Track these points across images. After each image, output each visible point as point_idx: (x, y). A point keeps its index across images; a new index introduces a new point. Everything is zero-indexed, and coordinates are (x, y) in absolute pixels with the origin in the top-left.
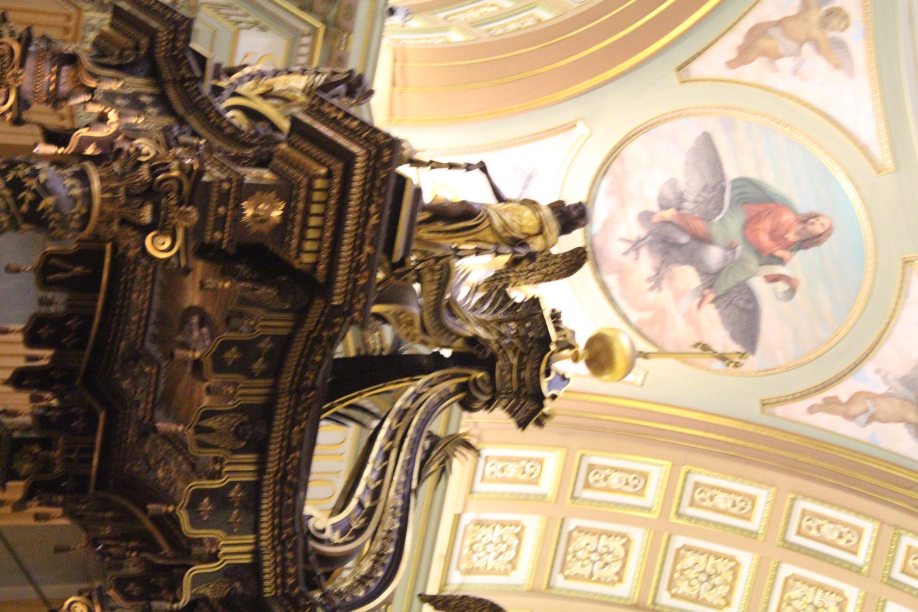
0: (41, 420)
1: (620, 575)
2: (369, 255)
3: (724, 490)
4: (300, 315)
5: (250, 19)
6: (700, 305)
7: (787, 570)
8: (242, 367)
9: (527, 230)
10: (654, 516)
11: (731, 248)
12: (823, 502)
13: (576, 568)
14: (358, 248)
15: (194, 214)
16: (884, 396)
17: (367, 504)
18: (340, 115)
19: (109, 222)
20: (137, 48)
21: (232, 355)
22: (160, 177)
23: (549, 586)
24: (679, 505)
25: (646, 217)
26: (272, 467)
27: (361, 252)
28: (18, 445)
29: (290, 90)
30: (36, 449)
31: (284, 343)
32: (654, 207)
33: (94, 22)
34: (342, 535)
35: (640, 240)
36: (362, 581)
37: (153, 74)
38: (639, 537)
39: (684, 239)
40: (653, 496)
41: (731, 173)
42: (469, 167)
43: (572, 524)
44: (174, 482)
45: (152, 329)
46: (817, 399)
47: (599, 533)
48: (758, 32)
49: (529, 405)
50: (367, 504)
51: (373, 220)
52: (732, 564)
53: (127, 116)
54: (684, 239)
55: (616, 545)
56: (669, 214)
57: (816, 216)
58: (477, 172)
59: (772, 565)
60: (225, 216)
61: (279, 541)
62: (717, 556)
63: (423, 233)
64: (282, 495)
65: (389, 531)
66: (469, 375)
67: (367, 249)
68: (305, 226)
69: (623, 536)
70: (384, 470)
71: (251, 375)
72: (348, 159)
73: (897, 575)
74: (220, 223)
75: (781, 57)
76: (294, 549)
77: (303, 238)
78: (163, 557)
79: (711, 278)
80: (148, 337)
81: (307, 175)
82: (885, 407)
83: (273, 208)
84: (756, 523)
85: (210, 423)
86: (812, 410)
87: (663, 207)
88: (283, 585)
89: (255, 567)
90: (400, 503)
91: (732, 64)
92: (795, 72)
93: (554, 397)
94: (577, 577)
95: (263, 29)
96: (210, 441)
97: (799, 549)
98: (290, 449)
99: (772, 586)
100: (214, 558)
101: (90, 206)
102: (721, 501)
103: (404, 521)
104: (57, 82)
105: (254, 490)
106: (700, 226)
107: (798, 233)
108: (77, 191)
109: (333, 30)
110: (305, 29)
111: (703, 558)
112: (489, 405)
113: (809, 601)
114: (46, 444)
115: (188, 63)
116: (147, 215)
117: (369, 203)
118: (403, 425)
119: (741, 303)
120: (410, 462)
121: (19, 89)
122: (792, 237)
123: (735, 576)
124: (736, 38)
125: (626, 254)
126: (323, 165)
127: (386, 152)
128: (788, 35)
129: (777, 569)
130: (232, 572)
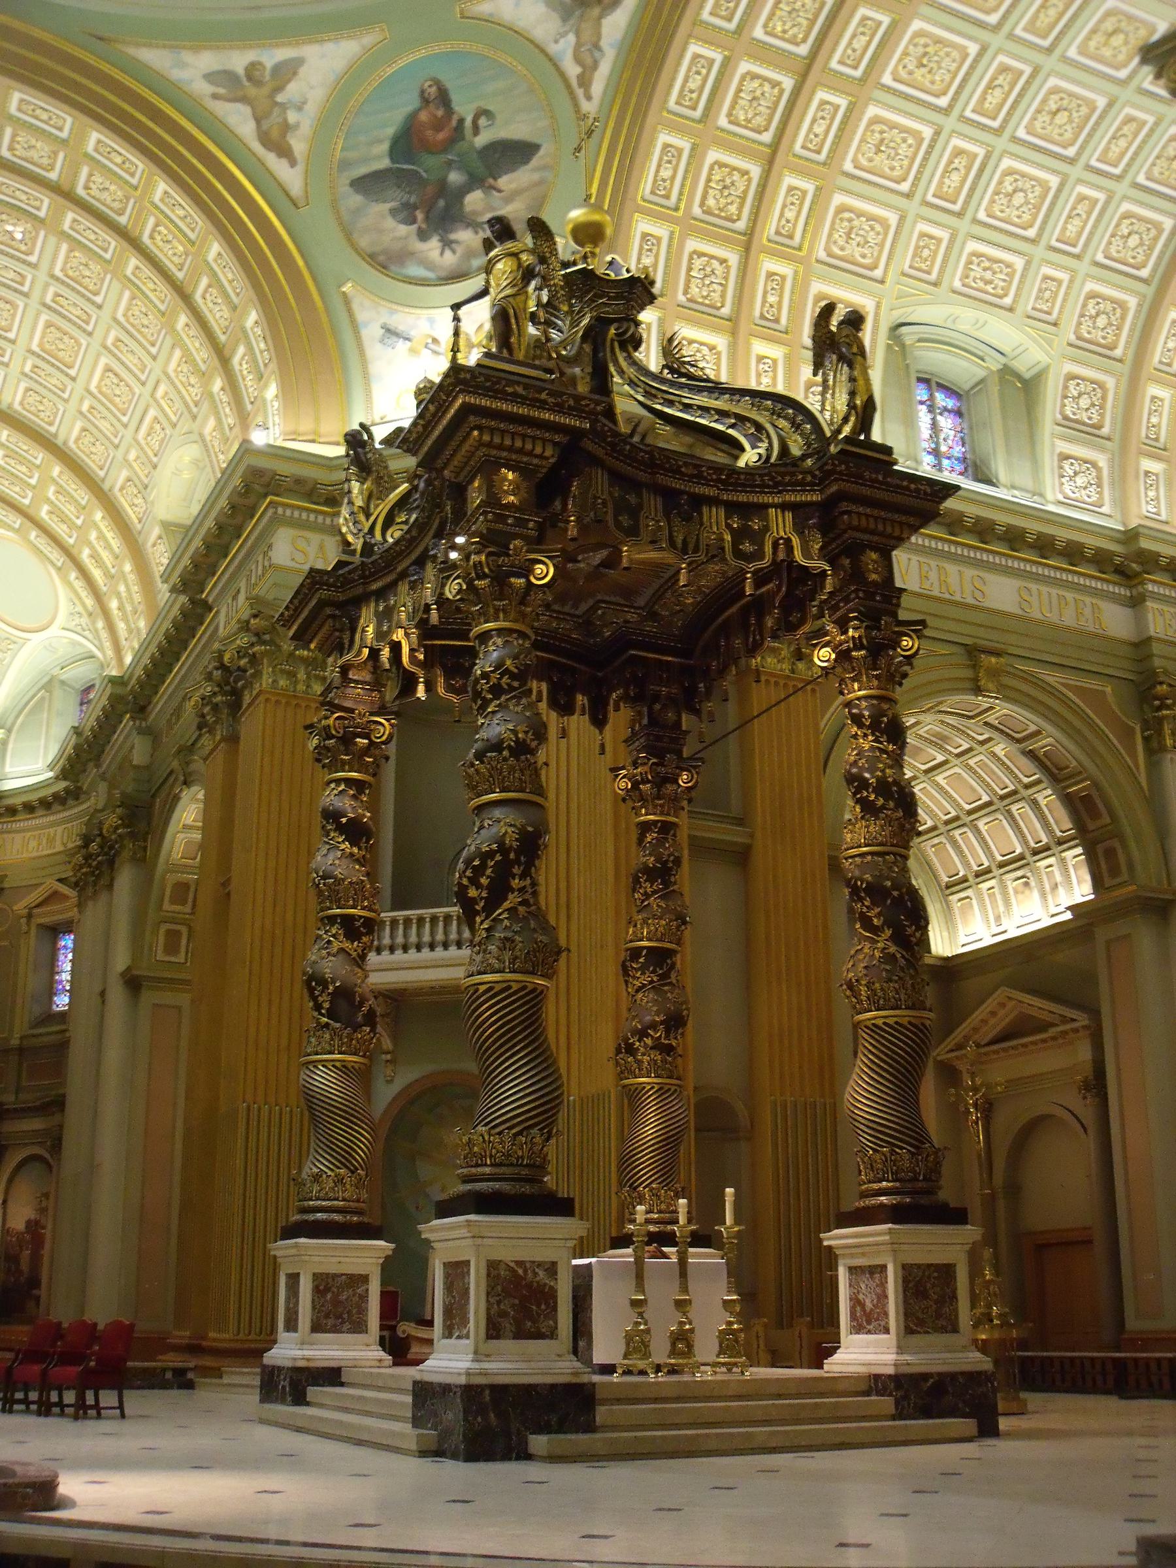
0: (633, 700)
1: (723, 261)
3: (657, 171)
4: (596, 461)
5: (260, 558)
6: (500, 191)
7: (723, 121)
8: (635, 512)
9: (515, 268)
10: (677, 229)
11: (449, 164)
12: (671, 86)
13: (716, 296)
14: (542, 405)
16: (578, 34)
18: (422, 422)
19: (524, 615)
20: (333, 616)
21: (625, 520)
22: (486, 570)
24: (668, 208)
25: (423, 236)
27: (545, 402)
28: (653, 722)
29: (361, 492)
30: (657, 707)
31: (616, 477)
32: (415, 227)
34: (762, 441)
35: (442, 240)
36: (796, 426)
37: (358, 601)
38: (692, 244)
39: (441, 203)
40: (660, 230)
41: (385, 163)
42: (457, 319)
43: (681, 298)
44: (699, 587)
45: (567, 609)
46: (580, 92)
47: (689, 278)
48: (265, 139)
49: (638, 290)
51: (520, 390)
52: (716, 167)
53: (399, 620)
54: (441, 203)
55: (698, 263)
56: (420, 216)
57: (423, 92)
58: (462, 312)
59: (718, 133)
61: (777, 487)
62: (709, 180)
63: (520, 355)
64: (736, 484)
65: (753, 404)
66: (612, 340)
67: (543, 396)
68: (521, 451)
69: (691, 258)
70: (700, 408)
71: (640, 506)
72: (466, 409)
73: (732, 26)
74: (520, 522)
75: (285, 120)
76: (783, 475)
78: (779, 587)
79: (475, 181)
80: (572, 611)
81: (477, 449)
82: (587, 36)
83: (505, 479)
84: (685, 144)
85: (679, 539)
86: (589, 98)
87: (414, 221)
88: (812, 484)
90: (727, 396)
91: (293, 163)
92: (300, 109)
93: (628, 271)
94: (723, 296)
95: (270, 546)
96: (694, 540)
97: (707, 109)
98: (699, 476)
99: (735, 134)
100: (788, 541)
101: (510, 631)
102: (666, 173)
103: (744, 392)
104: (362, 683)
106: (430, 190)
107: (438, 108)
108: (499, 641)
110: (270, 512)
111: (711, 191)
112: (637, 324)
113: (748, 104)
114: (656, 698)
116: (520, 582)
118: (660, 395)
119: (497, 156)
121: (372, 714)
122: (440, 113)
123: (726, 166)
124: (271, 159)
125: (454, 252)
126: (469, 434)
127: (462, 376)
128: (267, 115)
129: (723, 130)
130: (799, 528)
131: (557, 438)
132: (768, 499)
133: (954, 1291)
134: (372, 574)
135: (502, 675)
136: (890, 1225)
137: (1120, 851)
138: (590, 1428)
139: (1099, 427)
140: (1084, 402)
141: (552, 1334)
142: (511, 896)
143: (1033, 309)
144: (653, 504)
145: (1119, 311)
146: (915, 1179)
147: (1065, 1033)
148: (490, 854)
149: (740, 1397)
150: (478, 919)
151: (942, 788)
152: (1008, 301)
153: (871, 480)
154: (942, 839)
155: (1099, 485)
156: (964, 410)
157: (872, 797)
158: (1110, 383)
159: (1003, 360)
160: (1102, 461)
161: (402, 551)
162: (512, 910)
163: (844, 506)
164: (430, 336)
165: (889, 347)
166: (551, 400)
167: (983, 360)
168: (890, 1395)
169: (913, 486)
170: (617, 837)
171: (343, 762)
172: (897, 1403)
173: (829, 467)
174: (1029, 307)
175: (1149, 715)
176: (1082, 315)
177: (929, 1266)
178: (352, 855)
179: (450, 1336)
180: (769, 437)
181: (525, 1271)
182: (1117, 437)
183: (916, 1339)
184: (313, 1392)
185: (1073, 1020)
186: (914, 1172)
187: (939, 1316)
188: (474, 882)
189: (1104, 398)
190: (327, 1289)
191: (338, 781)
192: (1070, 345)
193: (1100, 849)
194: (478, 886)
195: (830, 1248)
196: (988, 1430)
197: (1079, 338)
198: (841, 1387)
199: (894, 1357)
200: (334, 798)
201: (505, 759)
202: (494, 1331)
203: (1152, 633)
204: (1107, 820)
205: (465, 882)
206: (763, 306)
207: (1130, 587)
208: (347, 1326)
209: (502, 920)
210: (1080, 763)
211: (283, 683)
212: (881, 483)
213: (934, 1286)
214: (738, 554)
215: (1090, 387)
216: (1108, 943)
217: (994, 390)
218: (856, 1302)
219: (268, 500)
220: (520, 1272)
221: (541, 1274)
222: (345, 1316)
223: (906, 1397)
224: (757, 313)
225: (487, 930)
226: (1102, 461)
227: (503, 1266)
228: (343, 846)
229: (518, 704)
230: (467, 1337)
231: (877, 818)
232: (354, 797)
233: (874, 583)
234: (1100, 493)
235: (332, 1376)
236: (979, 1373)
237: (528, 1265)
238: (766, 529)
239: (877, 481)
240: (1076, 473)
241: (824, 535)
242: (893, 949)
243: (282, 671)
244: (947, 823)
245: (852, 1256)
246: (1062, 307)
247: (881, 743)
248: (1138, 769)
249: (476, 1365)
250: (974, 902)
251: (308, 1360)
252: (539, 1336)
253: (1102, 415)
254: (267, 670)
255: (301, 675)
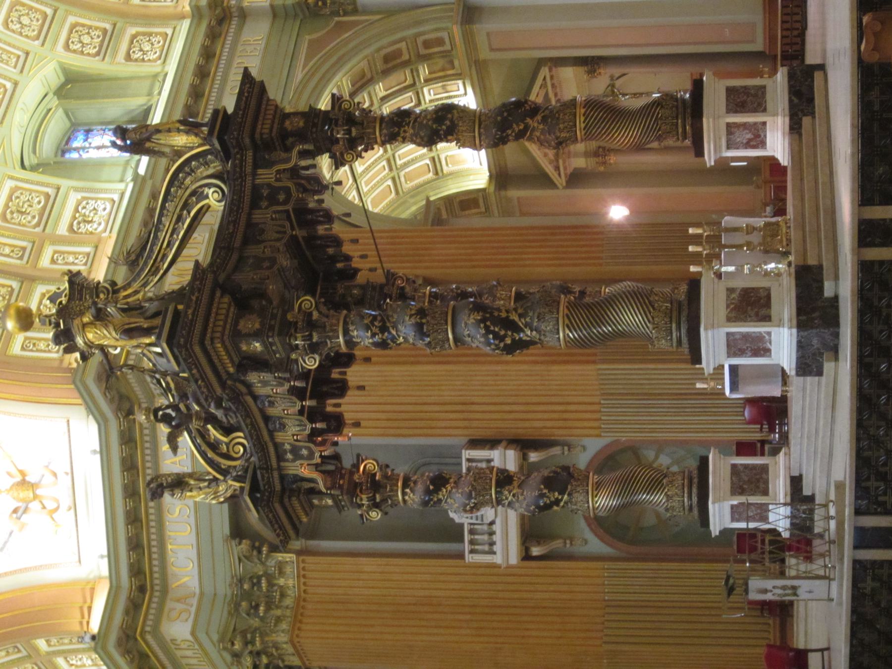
2: (193, 295)
4: (228, 277)
15: (289, 317)
17: (185, 212)
21: (266, 264)
23: (22, 283)
26: (244, 217)
27: (197, 298)
33: (282, 635)
50: (185, 212)
51: (190, 312)
60: (271, 320)
61: (242, 177)
65: (172, 201)
67: (194, 298)
70: (172, 235)
77: (227, 316)
85: (278, 236)
89: (256, 166)
90: (163, 219)
100: (278, 172)
101: (346, 323)
105: (255, 204)
109: (130, 633)
115: (263, 480)
117: (192, 320)
118: (157, 264)
120: (153, 245)
130: (269, 164)
131: (218, 294)
132: (249, 183)
133: (742, 87)
134: (266, 463)
135: (373, 325)
136: (704, 120)
137: (427, 37)
138: (820, 267)
139: (105, 31)
140: (86, 39)
141: (768, 290)
142: (511, 318)
143: (15, 67)
144: (254, 250)
145: (18, 7)
146: (677, 107)
147: (553, 86)
148: (487, 328)
149: (802, 200)
150: (525, 338)
151: (367, 169)
152: (9, 85)
153: (242, 118)
154: (402, 174)
155: (150, 34)
156: (87, 128)
157: (444, 127)
158: (71, 19)
159: (51, 95)
160: (133, 30)
161: (257, 435)
162: (520, 316)
163: (257, 136)
164: (11, 515)
165: (42, 173)
166: (196, 294)
167: (50, 109)
168: (801, 119)
169: (246, 94)
170: (418, 363)
171: (391, 490)
172: (805, 115)
173: (234, 142)
174: (14, 70)
175: (327, 11)
176: (21, 34)
177: (727, 100)
178: (455, 483)
179: (769, 351)
180: (201, 187)
181: (733, 303)
182: (114, 19)
183: (769, 106)
184: (806, 492)
185: (545, 79)
186: (673, 107)
187: (756, 95)
188: (502, 339)
189: (83, 25)
190: (741, 487)
191: (404, 494)
192: (43, 45)
193: (423, 51)
194: (505, 336)
195: (715, 161)
196: (822, 67)
197: (37, 38)
198: (797, 148)
199: (779, 118)
200: (414, 498)
201: (428, 322)
202: (767, 318)
203: (268, 4)
204: (403, 45)
205: (502, 345)
206: (12, 257)
207: (231, 17)
208: (764, 476)
209: (526, 322)
210: (363, 59)
211: (284, 626)
212: (244, 111)
213: (739, 98)
214: (286, 202)
215: (74, 35)
216: (492, 50)
217: (73, 104)
218: (748, 145)
219: (139, 638)
220: (732, 306)
221: (733, 296)
222: (758, 477)
223: (802, 111)
224: (18, 262)
225: (532, 331)
226: (133, 30)
227: (730, 315)
228: (449, 488)
229: (392, 316)
230: (769, 334)
231: (457, 125)
232: (415, 482)
233: (304, 123)
234: (157, 34)
235: (796, 482)
236: (789, 73)
237: (729, 302)
238: (269, 185)
239: (243, 115)
240: (141, 50)
241: (275, 149)
242: (539, 117)
243: (275, 625)
244: (391, 169)
245: (720, 147)
246: (14, 47)
247: (410, 122)
248: (367, 21)
249: (786, 325)
250: (449, 153)
251: (786, 495)
252: (769, 297)
253: (96, 28)
254: (274, 637)
255: (278, 612)
